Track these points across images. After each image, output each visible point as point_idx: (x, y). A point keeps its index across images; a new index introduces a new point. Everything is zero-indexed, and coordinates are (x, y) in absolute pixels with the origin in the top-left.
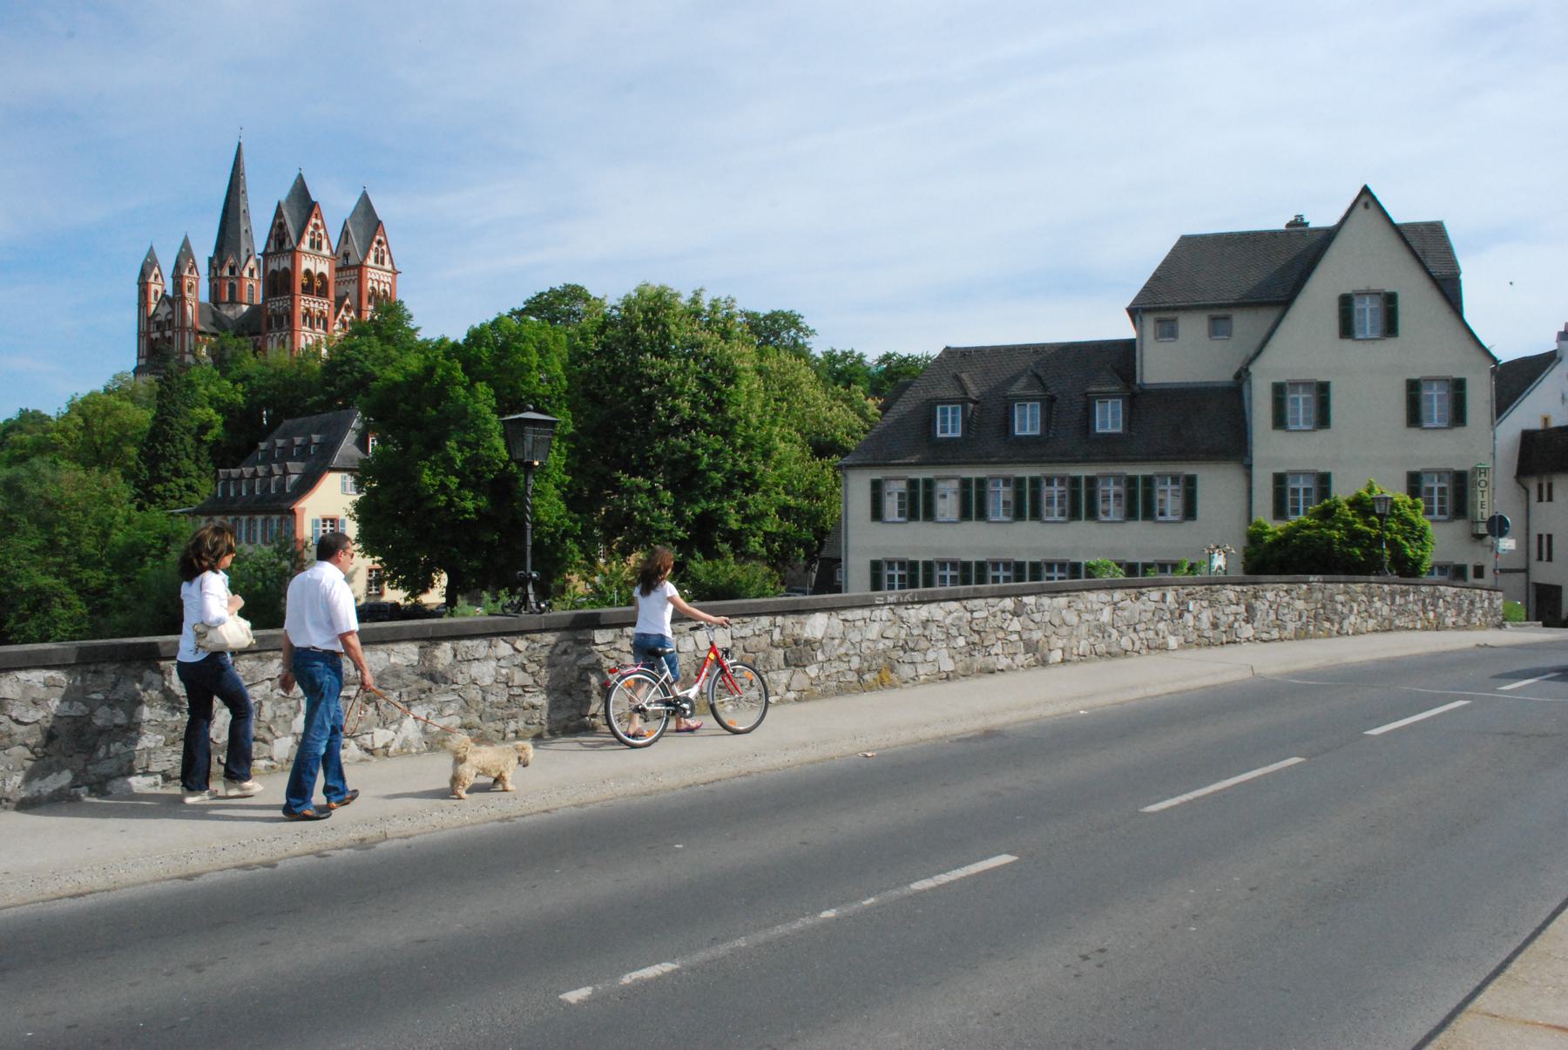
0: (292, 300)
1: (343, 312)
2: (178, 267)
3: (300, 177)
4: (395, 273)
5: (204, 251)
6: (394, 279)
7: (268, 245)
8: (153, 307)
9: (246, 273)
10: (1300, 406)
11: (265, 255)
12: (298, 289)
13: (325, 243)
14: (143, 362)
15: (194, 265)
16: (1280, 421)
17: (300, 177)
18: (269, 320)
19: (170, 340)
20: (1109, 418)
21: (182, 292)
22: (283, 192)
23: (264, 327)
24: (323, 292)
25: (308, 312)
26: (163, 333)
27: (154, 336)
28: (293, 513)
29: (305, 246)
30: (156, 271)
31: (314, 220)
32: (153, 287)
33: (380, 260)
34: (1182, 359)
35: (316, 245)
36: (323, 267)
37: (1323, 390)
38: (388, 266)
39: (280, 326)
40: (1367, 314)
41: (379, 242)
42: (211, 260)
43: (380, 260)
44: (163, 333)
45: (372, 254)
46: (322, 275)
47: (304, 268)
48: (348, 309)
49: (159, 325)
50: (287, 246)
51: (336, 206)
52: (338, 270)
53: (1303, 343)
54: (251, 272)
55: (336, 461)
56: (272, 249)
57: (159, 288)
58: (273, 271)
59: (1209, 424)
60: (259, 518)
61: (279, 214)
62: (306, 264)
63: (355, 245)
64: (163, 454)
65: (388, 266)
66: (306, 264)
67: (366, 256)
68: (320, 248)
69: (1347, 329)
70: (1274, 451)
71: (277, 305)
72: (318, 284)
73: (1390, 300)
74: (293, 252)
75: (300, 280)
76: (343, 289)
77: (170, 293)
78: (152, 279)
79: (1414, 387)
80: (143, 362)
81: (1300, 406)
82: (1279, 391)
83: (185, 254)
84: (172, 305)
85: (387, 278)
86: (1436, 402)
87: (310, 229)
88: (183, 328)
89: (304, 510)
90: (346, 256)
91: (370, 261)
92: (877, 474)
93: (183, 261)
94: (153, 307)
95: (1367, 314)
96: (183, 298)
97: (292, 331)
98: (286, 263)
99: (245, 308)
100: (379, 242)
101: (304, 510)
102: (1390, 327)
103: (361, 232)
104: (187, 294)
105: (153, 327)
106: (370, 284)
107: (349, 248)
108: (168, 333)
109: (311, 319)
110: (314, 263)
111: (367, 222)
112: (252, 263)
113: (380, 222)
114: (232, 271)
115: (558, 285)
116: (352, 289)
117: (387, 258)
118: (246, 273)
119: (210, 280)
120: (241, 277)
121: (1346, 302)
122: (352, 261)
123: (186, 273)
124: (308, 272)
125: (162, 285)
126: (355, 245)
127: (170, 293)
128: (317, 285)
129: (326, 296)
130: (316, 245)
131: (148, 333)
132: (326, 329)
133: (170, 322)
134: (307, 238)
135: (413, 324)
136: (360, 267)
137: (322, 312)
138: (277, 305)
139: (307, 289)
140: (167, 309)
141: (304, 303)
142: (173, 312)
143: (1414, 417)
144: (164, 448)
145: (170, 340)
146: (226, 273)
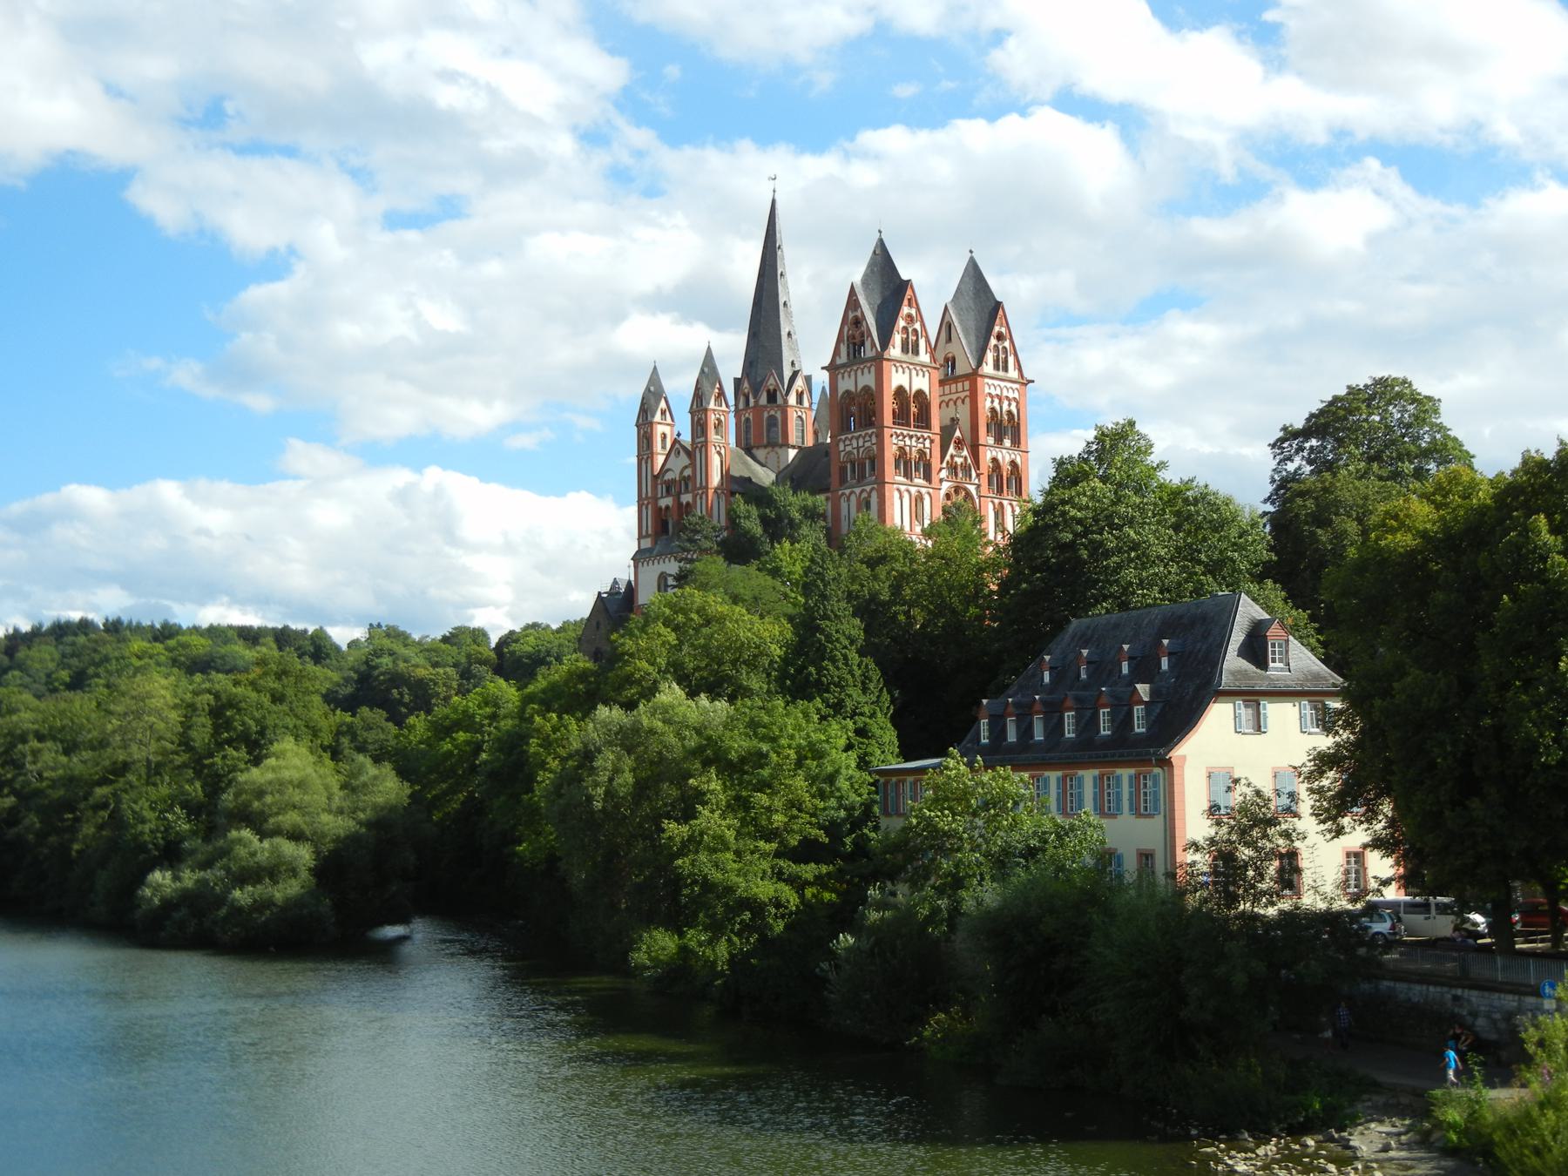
0: (880, 436)
1: (951, 450)
2: (699, 397)
3: (881, 241)
4: (1025, 382)
5: (731, 368)
8: (660, 460)
9: (792, 399)
11: (832, 368)
12: (888, 419)
13: (922, 342)
14: (647, 543)
15: (721, 394)
17: (881, 241)
18: (843, 470)
21: (704, 432)
22: (857, 272)
27: (666, 502)
28: (1166, 764)
29: (895, 351)
30: (663, 405)
31: (905, 310)
32: (660, 430)
33: (1001, 364)
35: (910, 347)
36: (921, 383)
38: (1013, 373)
39: (861, 478)
41: (1000, 337)
42: (738, 382)
43: (1001, 364)
45: (990, 356)
46: (920, 393)
47: (894, 385)
49: (669, 485)
50: (868, 352)
51: (933, 285)
52: (942, 383)
54: (800, 396)
55: (1226, 681)
56: (843, 359)
57: (667, 430)
58: (847, 392)
60: (1088, 776)
61: (852, 303)
62: (897, 378)
63: (963, 347)
64: (818, 682)
65: (1013, 373)
66: (897, 378)
68: (916, 352)
71: (854, 444)
72: (913, 409)
74: (879, 360)
75: (889, 405)
76: (950, 412)
78: (658, 417)
80: (647, 543)
83: (709, 369)
84: (690, 454)
87: (901, 323)
89: (1184, 758)
90: (951, 362)
91: (988, 368)
93: (706, 385)
94: (660, 460)
96: (705, 444)
97: (881, 483)
98: (867, 379)
99: (792, 453)
100: (1000, 337)
101: (1184, 758)
103: (972, 324)
104: (713, 436)
107: (953, 349)
109: (907, 463)
110: (907, 375)
112: (799, 384)
113: (998, 305)
114: (772, 397)
115: (1362, 379)
116: (963, 413)
117: (1011, 360)
118: (792, 399)
119: (737, 413)
120: (784, 408)
122: (961, 369)
123: (712, 405)
124: (900, 391)
125: (674, 426)
127: (686, 438)
128: (913, 410)
130: (910, 347)
131: (655, 499)
133: (686, 482)
134: (897, 338)
135: (1153, 459)
136: (973, 376)
137: (921, 453)
138: (854, 444)
140: (684, 460)
141: (895, 440)
142: (693, 465)
144: (820, 670)
146: (763, 400)
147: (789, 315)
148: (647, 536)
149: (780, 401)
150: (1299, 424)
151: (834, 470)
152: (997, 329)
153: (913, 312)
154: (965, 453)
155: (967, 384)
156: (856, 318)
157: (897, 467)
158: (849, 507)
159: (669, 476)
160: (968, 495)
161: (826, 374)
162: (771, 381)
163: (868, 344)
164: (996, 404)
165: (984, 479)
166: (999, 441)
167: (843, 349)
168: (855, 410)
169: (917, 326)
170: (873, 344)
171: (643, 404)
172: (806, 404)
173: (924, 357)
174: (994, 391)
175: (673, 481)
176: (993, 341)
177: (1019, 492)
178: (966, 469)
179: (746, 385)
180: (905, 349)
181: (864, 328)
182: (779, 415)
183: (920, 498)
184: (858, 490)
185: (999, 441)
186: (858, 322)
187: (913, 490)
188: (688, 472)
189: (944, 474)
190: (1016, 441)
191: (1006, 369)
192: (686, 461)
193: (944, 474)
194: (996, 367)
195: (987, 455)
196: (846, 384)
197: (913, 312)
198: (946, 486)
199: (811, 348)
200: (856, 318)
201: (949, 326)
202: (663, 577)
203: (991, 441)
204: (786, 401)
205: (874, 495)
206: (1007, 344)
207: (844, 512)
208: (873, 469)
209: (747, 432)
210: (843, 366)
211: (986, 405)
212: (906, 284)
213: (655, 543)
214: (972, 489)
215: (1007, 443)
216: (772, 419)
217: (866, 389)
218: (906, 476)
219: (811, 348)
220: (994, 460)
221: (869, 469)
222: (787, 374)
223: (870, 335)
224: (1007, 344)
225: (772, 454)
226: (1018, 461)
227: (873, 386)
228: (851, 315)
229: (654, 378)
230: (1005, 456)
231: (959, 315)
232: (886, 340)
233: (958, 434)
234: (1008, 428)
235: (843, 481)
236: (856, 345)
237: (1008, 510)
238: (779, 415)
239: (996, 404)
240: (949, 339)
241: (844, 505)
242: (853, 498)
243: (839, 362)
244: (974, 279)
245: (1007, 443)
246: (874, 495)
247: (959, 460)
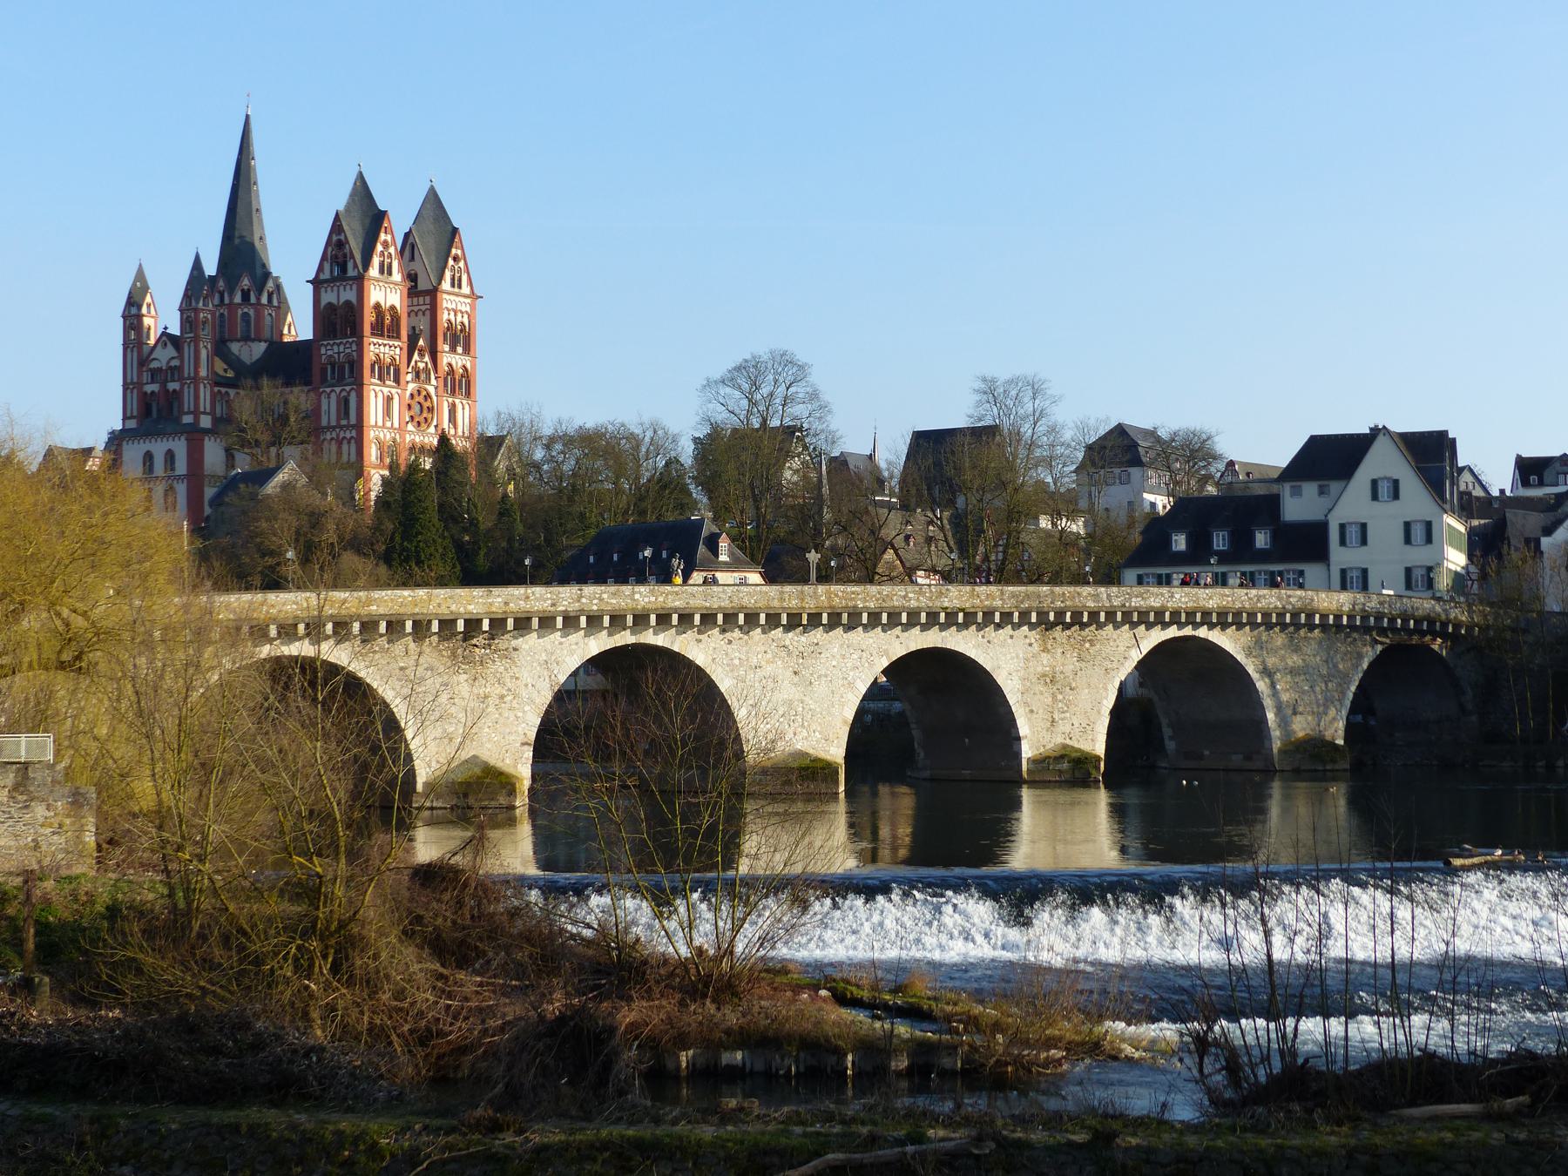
1: (416, 357)
2: (187, 296)
3: (361, 176)
4: (474, 296)
5: (210, 268)
6: (473, 307)
7: (320, 269)
9: (264, 300)
10: (1353, 533)
11: (316, 283)
16: (1343, 542)
17: (361, 176)
18: (324, 370)
19: (177, 395)
20: (1261, 539)
22: (339, 198)
23: (316, 377)
24: (394, 333)
25: (378, 360)
26: (164, 385)
27: (149, 388)
29: (374, 272)
30: (148, 299)
31: (383, 236)
34: (1299, 506)
35: (385, 270)
37: (1364, 526)
38: (466, 290)
39: (340, 381)
40: (1384, 489)
44: (164, 385)
45: (448, 274)
46: (393, 308)
47: (373, 301)
48: (421, 355)
49: (155, 374)
50: (351, 272)
53: (1352, 502)
54: (270, 295)
56: (326, 275)
59: (1306, 545)
61: (337, 227)
65: (466, 290)
67: (441, 278)
68: (390, 273)
69: (1375, 497)
70: (1340, 557)
71: (332, 350)
73: (1396, 483)
74: (360, 280)
75: (369, 318)
77: (175, 330)
79: (1407, 525)
80: (132, 424)
81: (1353, 533)
82: (1342, 527)
85: (464, 305)
86: (1418, 533)
87: (379, 248)
88: (196, 379)
91: (446, 285)
92: (1141, 571)
95: (1384, 489)
96: (196, 340)
97: (359, 386)
98: (349, 295)
100: (456, 259)
102: (1396, 495)
105: (146, 377)
106: (445, 317)
107: (416, 266)
108: (173, 386)
111: (438, 232)
112: (270, 285)
113: (455, 231)
114: (246, 296)
116: (423, 324)
118: (264, 300)
121: (1374, 483)
124: (377, 306)
125: (163, 317)
126: (426, 258)
127: (175, 330)
128: (386, 325)
129: (398, 337)
130: (385, 270)
131: (139, 385)
132: (397, 380)
133: (174, 372)
134: (376, 260)
136: (433, 293)
138: (332, 350)
139: (378, 329)
140: (171, 351)
141: (377, 349)
142: (181, 357)
143: (1408, 540)
145: (177, 395)
146: (238, 299)
147: (261, 221)
148: (132, 417)
149: (253, 300)
150: (717, 376)
151: (316, 371)
152: (454, 251)
153: (389, 238)
154: (427, 359)
155: (428, 299)
156: (339, 241)
157: (373, 370)
158: (329, 407)
159: (154, 365)
160: (428, 397)
161: (310, 286)
162: (246, 282)
163: (350, 265)
164: (452, 317)
165: (441, 381)
166: (453, 350)
167: (327, 266)
168: (340, 319)
169: (392, 250)
170: (355, 266)
171: (130, 297)
172: (275, 303)
173: (397, 276)
174: (452, 306)
175: (160, 370)
176: (451, 262)
177: (468, 394)
178: (426, 370)
179: (221, 283)
180: (382, 271)
181: (347, 250)
182: (252, 312)
183: (389, 399)
184: (338, 389)
185: (453, 350)
186: (341, 245)
187: (386, 390)
188: (175, 363)
189: (409, 377)
190: (467, 350)
191: (460, 287)
192: (173, 353)
193: (409, 377)
194: (453, 285)
195: (447, 358)
196: (328, 297)
197: (389, 238)
198: (411, 387)
199: (293, 257)
200: (339, 241)
201: (413, 247)
202: (148, 457)
203: (447, 348)
204: (258, 299)
205: (353, 394)
206: (462, 264)
207: (324, 407)
208: (352, 371)
209: (222, 326)
210: (326, 281)
211: (444, 317)
212: (381, 215)
213: (140, 423)
214: (431, 390)
215: (460, 350)
216: (246, 315)
217: (348, 303)
218: (380, 378)
219: (293, 257)
220: (450, 365)
221: (350, 373)
222: (259, 271)
223: (352, 257)
224: (462, 264)
225: (246, 348)
226: (468, 366)
227: (354, 300)
228: (335, 238)
229: (140, 275)
230: (458, 360)
231: (421, 237)
232: (367, 263)
233: (421, 342)
234: (462, 338)
235: (324, 381)
236: (342, 262)
237: (459, 407)
238: (252, 312)
239: (452, 317)
240: (412, 258)
241: (324, 401)
242: (333, 396)
243: (322, 277)
244: (433, 201)
245: (460, 350)
246: (353, 394)
247: (421, 365)
